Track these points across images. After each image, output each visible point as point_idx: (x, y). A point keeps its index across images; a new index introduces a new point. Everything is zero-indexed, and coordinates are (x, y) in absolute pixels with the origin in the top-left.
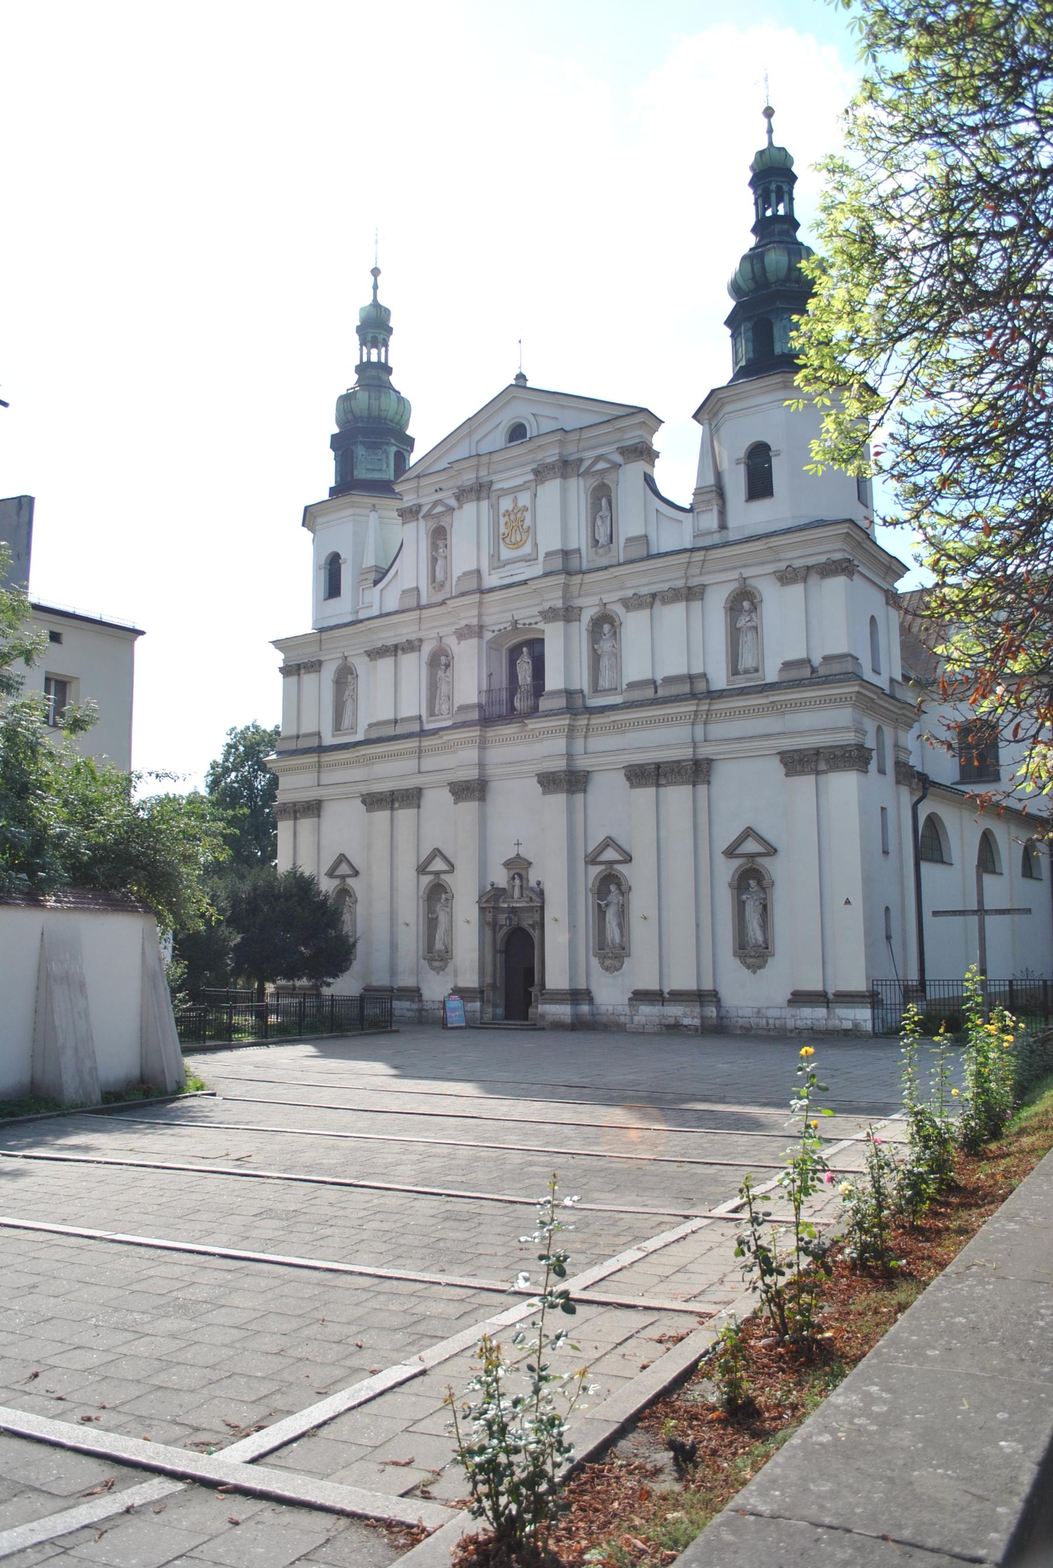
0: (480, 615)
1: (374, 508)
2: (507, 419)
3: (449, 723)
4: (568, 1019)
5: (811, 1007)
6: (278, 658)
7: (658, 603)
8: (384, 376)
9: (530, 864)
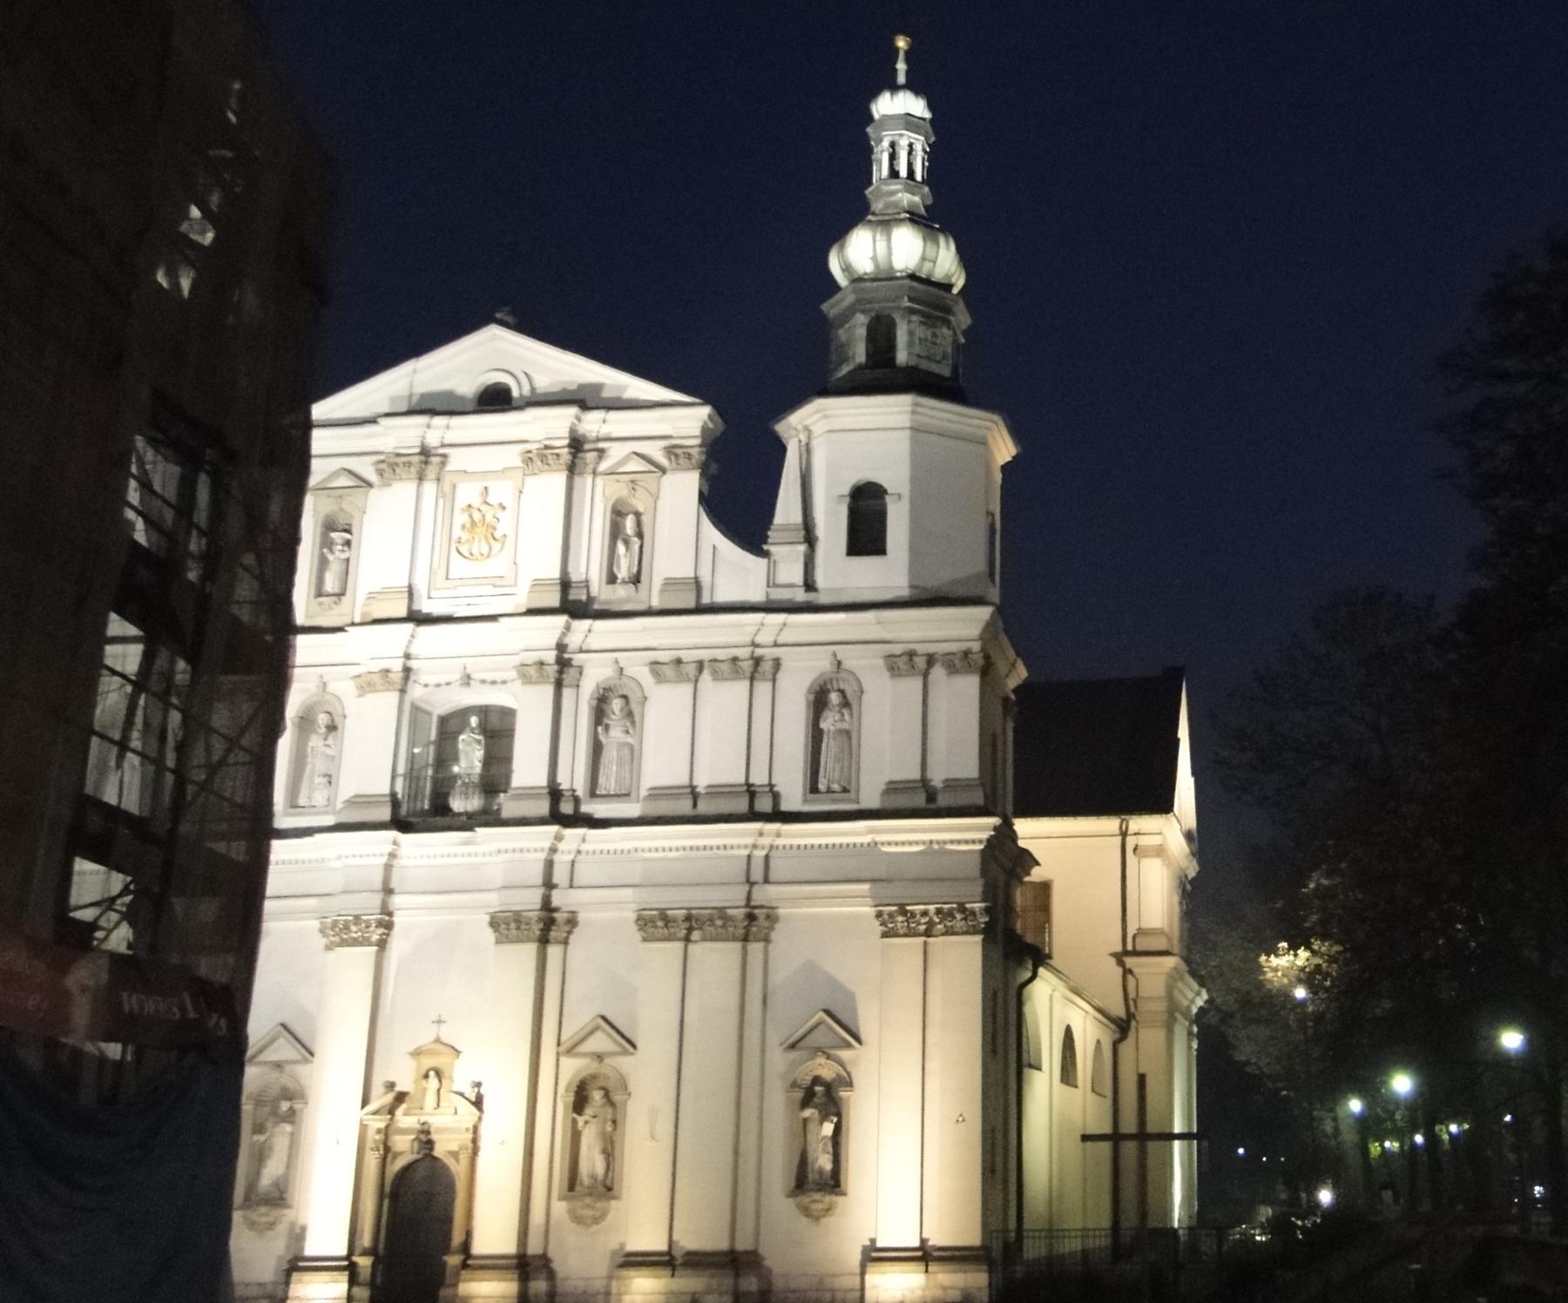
7: (706, 676)
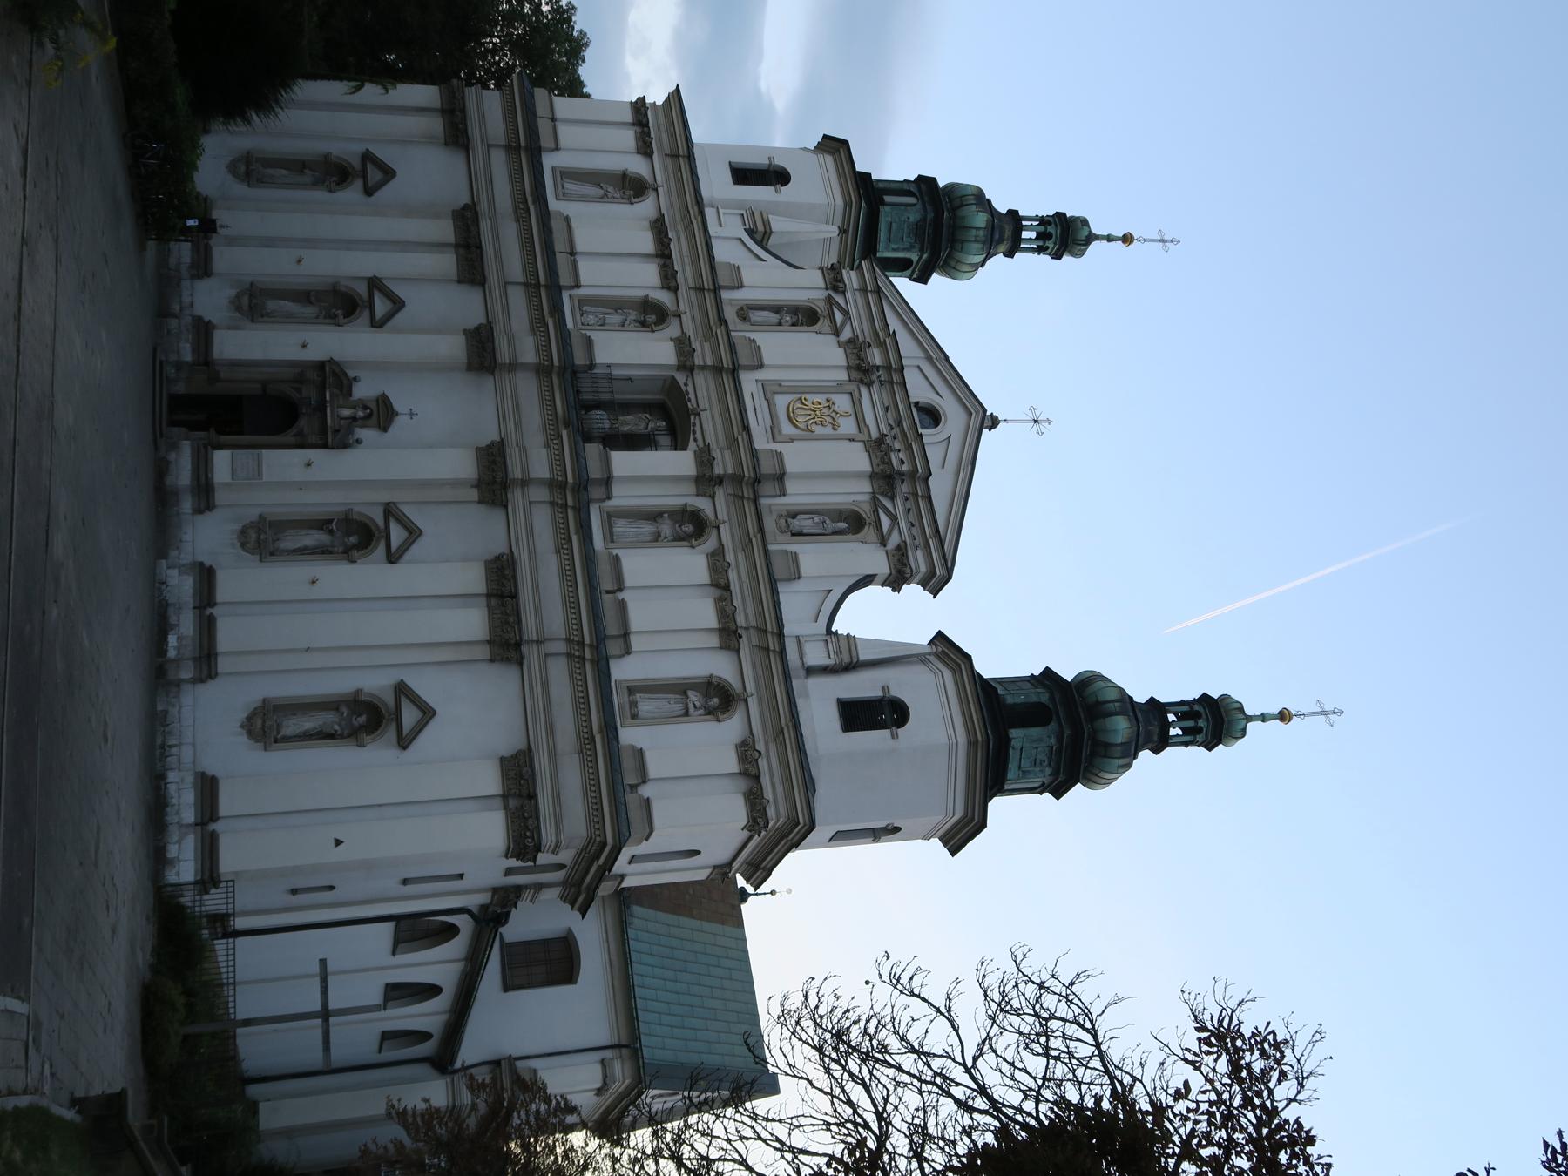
0: (704, 367)
1: (843, 231)
2: (948, 405)
3: (570, 325)
4: (169, 481)
5: (195, 804)
6: (657, 96)
7: (717, 593)
8: (1003, 247)
9: (385, 430)
